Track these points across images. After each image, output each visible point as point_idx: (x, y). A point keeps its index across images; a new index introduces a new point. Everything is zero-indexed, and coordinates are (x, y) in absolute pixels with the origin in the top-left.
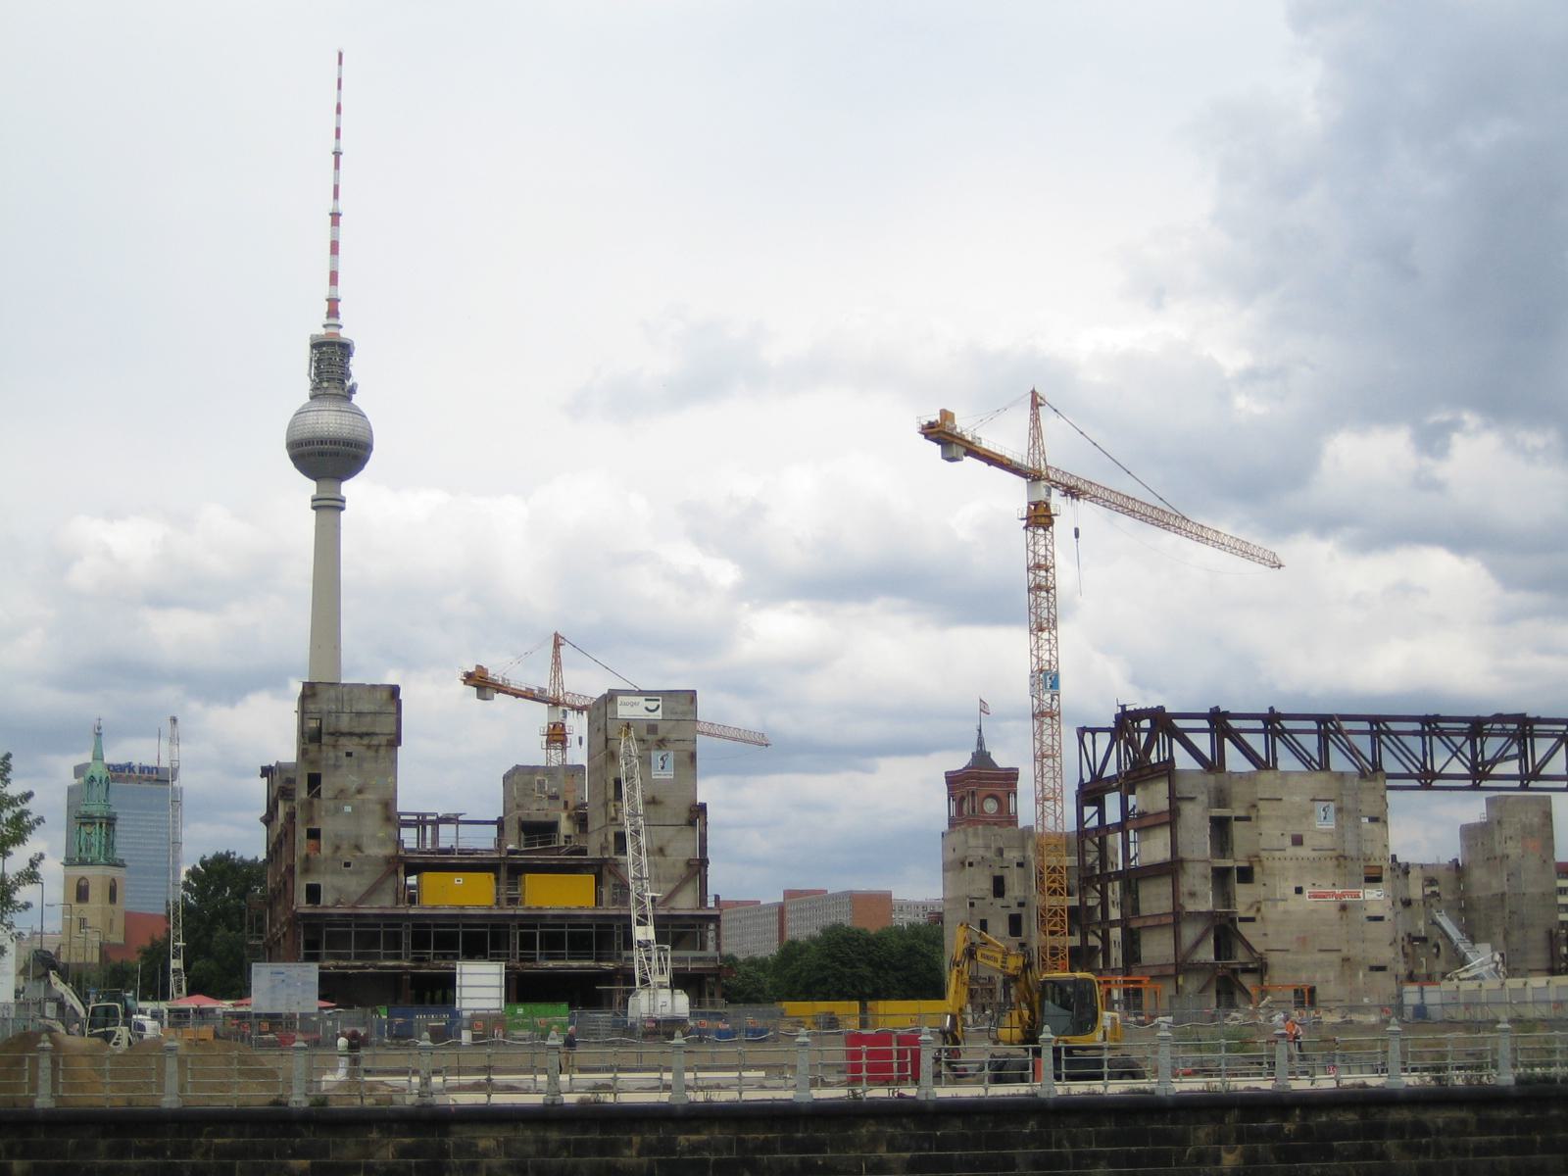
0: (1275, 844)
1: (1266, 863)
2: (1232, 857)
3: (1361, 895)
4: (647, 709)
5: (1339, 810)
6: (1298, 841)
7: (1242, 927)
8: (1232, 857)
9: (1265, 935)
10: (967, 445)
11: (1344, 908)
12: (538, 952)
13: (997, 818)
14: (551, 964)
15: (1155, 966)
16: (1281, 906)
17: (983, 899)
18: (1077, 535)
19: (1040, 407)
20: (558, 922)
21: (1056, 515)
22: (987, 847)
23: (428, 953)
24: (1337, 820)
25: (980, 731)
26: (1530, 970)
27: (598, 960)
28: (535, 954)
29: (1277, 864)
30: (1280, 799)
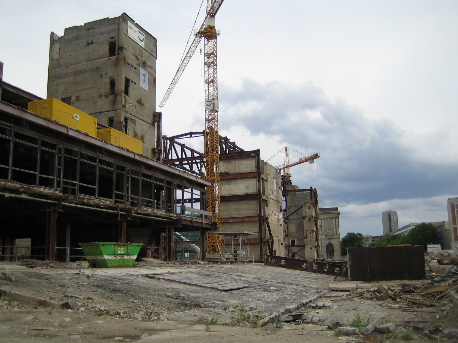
4: (139, 37)
14: (149, 210)
23: (74, 185)
28: (138, 199)
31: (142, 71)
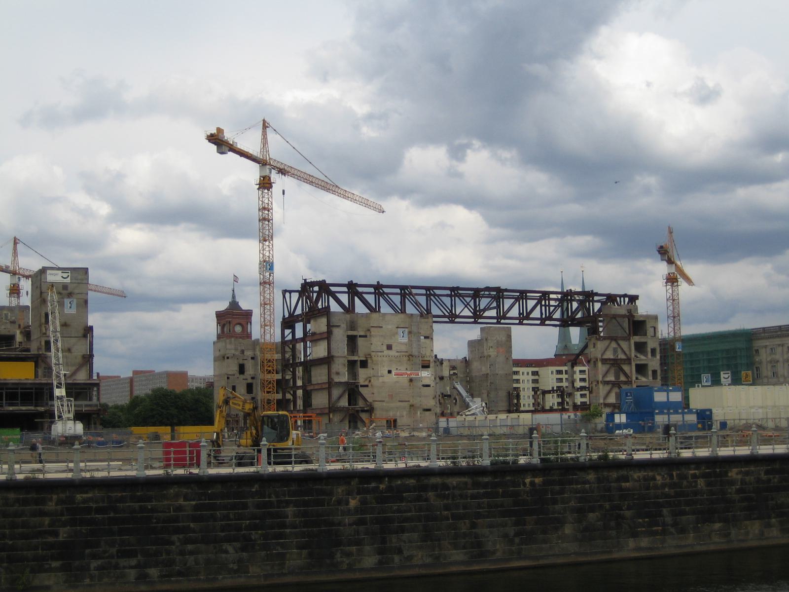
0: (379, 349)
1: (374, 358)
2: (357, 355)
3: (420, 374)
4: (62, 277)
5: (410, 333)
6: (389, 347)
7: (361, 389)
8: (357, 355)
9: (373, 393)
10: (230, 146)
11: (411, 380)
12: (4, 402)
13: (242, 335)
14: (11, 408)
15: (318, 409)
16: (381, 379)
17: (234, 375)
18: (284, 193)
19: (267, 128)
20: (15, 386)
21: (274, 183)
22: (236, 349)
24: (409, 338)
25: (233, 291)
26: (499, 411)
27: (36, 406)
28: (3, 403)
29: (380, 359)
30: (382, 327)
31: (67, 301)
